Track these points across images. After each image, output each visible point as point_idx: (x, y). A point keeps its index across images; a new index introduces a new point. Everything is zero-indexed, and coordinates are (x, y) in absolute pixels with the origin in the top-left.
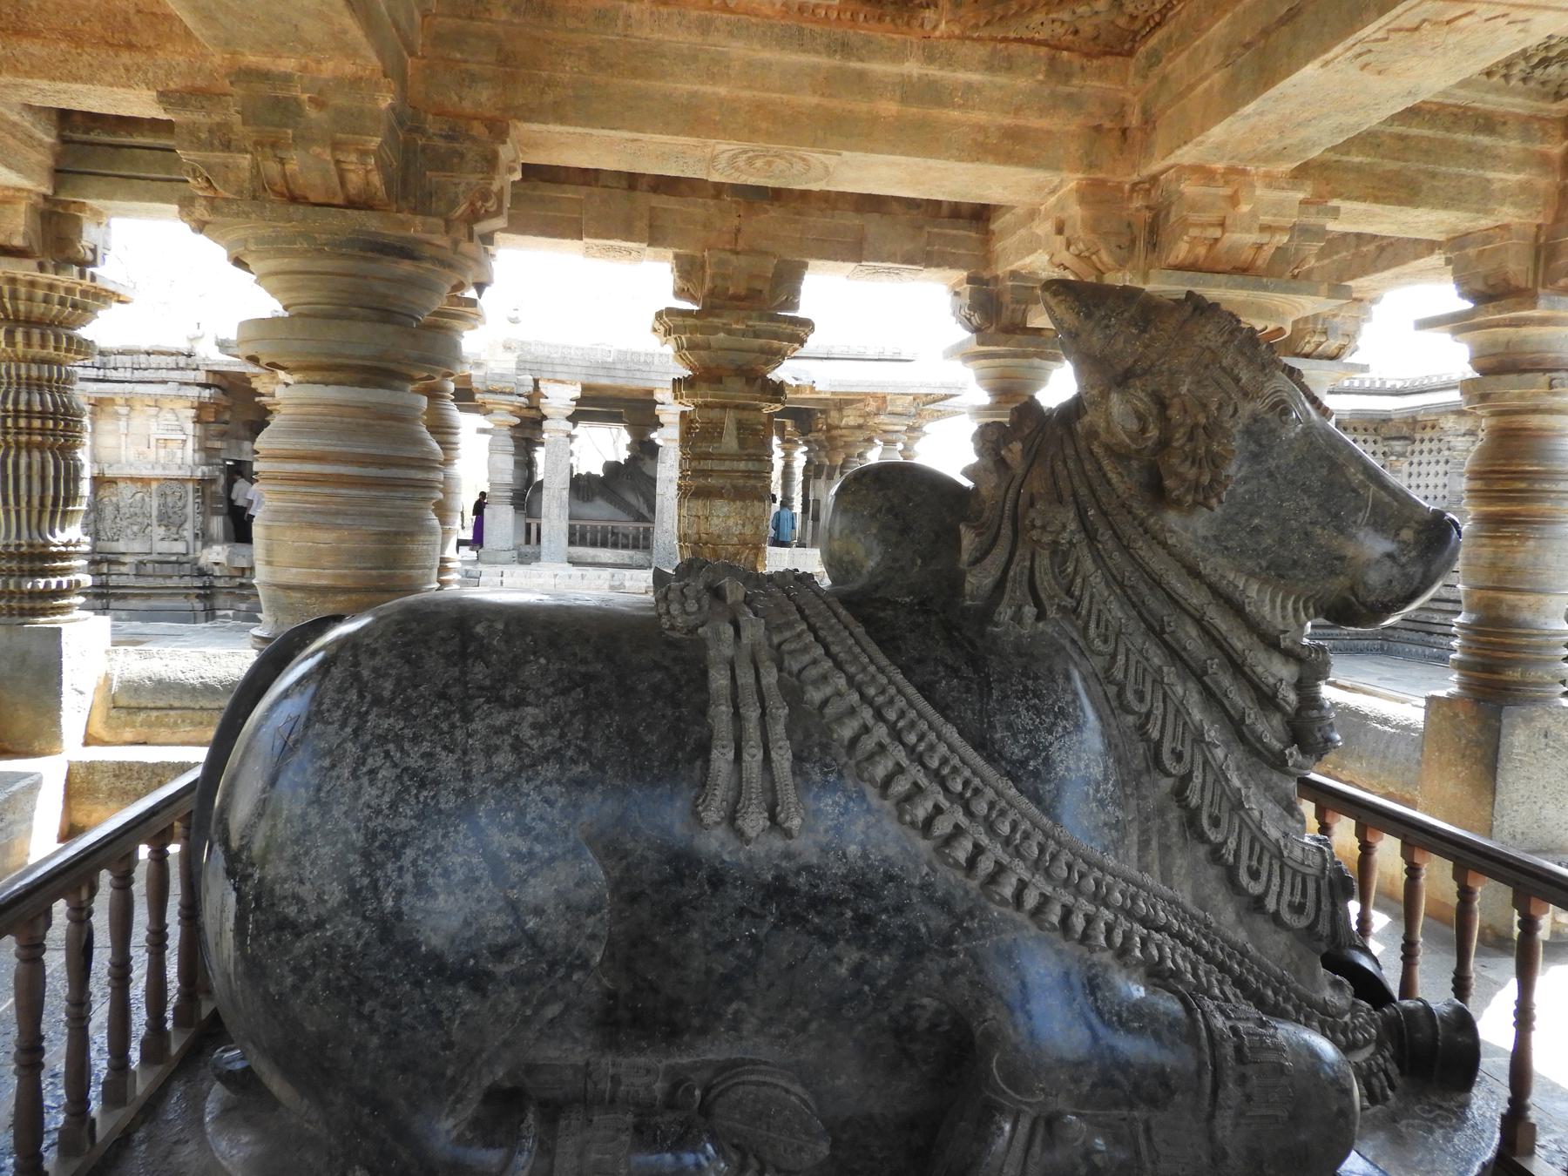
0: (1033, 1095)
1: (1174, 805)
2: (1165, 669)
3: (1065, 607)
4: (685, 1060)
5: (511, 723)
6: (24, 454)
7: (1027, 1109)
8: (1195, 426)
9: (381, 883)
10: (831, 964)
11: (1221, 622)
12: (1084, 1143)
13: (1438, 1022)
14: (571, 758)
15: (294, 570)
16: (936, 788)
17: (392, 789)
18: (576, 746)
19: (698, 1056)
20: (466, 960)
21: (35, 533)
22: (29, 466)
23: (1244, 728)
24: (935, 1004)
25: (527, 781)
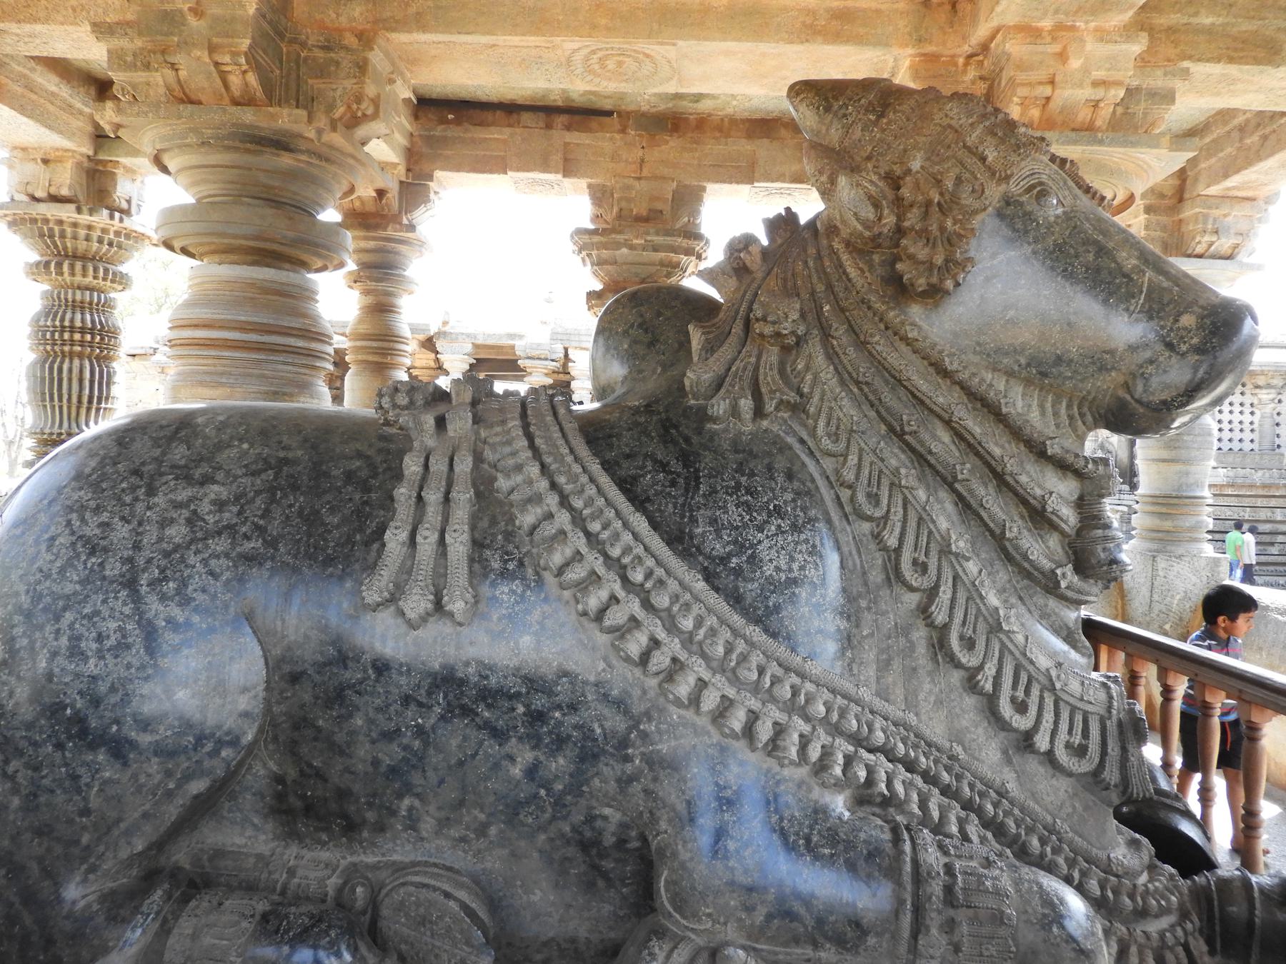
1: (920, 623)
2: (903, 471)
4: (370, 859)
5: (191, 500)
6: (67, 360)
7: (693, 936)
8: (928, 204)
9: (38, 644)
10: (504, 763)
11: (975, 426)
13: (1256, 894)
16: (612, 576)
18: (253, 523)
19: (383, 855)
21: (74, 425)
22: (70, 370)
23: (1007, 544)
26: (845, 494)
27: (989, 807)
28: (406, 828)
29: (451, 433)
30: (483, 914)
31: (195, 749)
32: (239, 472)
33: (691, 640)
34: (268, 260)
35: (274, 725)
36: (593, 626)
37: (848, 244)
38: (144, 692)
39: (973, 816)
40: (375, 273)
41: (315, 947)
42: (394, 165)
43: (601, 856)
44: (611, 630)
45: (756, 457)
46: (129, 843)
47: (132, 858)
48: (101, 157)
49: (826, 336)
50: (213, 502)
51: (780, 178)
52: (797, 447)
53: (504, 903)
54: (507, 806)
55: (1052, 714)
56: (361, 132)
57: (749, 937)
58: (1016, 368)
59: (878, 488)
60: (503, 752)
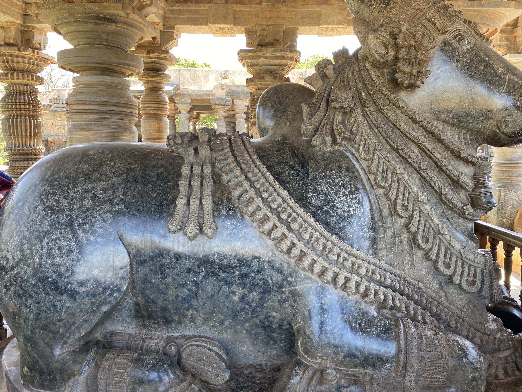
0: (316, 359)
1: (405, 231)
2: (398, 166)
3: (347, 138)
4: (175, 334)
6: (19, 117)
8: (410, 46)
9: (34, 252)
11: (429, 145)
12: (337, 382)
14: (116, 203)
19: (181, 333)
20: (67, 285)
22: (21, 122)
23: (443, 196)
24: (279, 316)
25: (96, 212)
27: (434, 308)
28: (190, 322)
29: (201, 155)
30: (224, 356)
31: (103, 294)
32: (111, 176)
33: (308, 243)
34: (108, 73)
36: (266, 238)
37: (372, 64)
39: (427, 312)
40: (152, 73)
41: (158, 372)
42: (157, 24)
43: (272, 332)
44: (274, 239)
45: (333, 162)
46: (79, 332)
49: (363, 106)
50: (102, 189)
51: (332, 23)
52: (351, 157)
53: (231, 351)
54: (232, 312)
56: (145, 12)
57: (336, 365)
58: (448, 119)
60: (230, 291)
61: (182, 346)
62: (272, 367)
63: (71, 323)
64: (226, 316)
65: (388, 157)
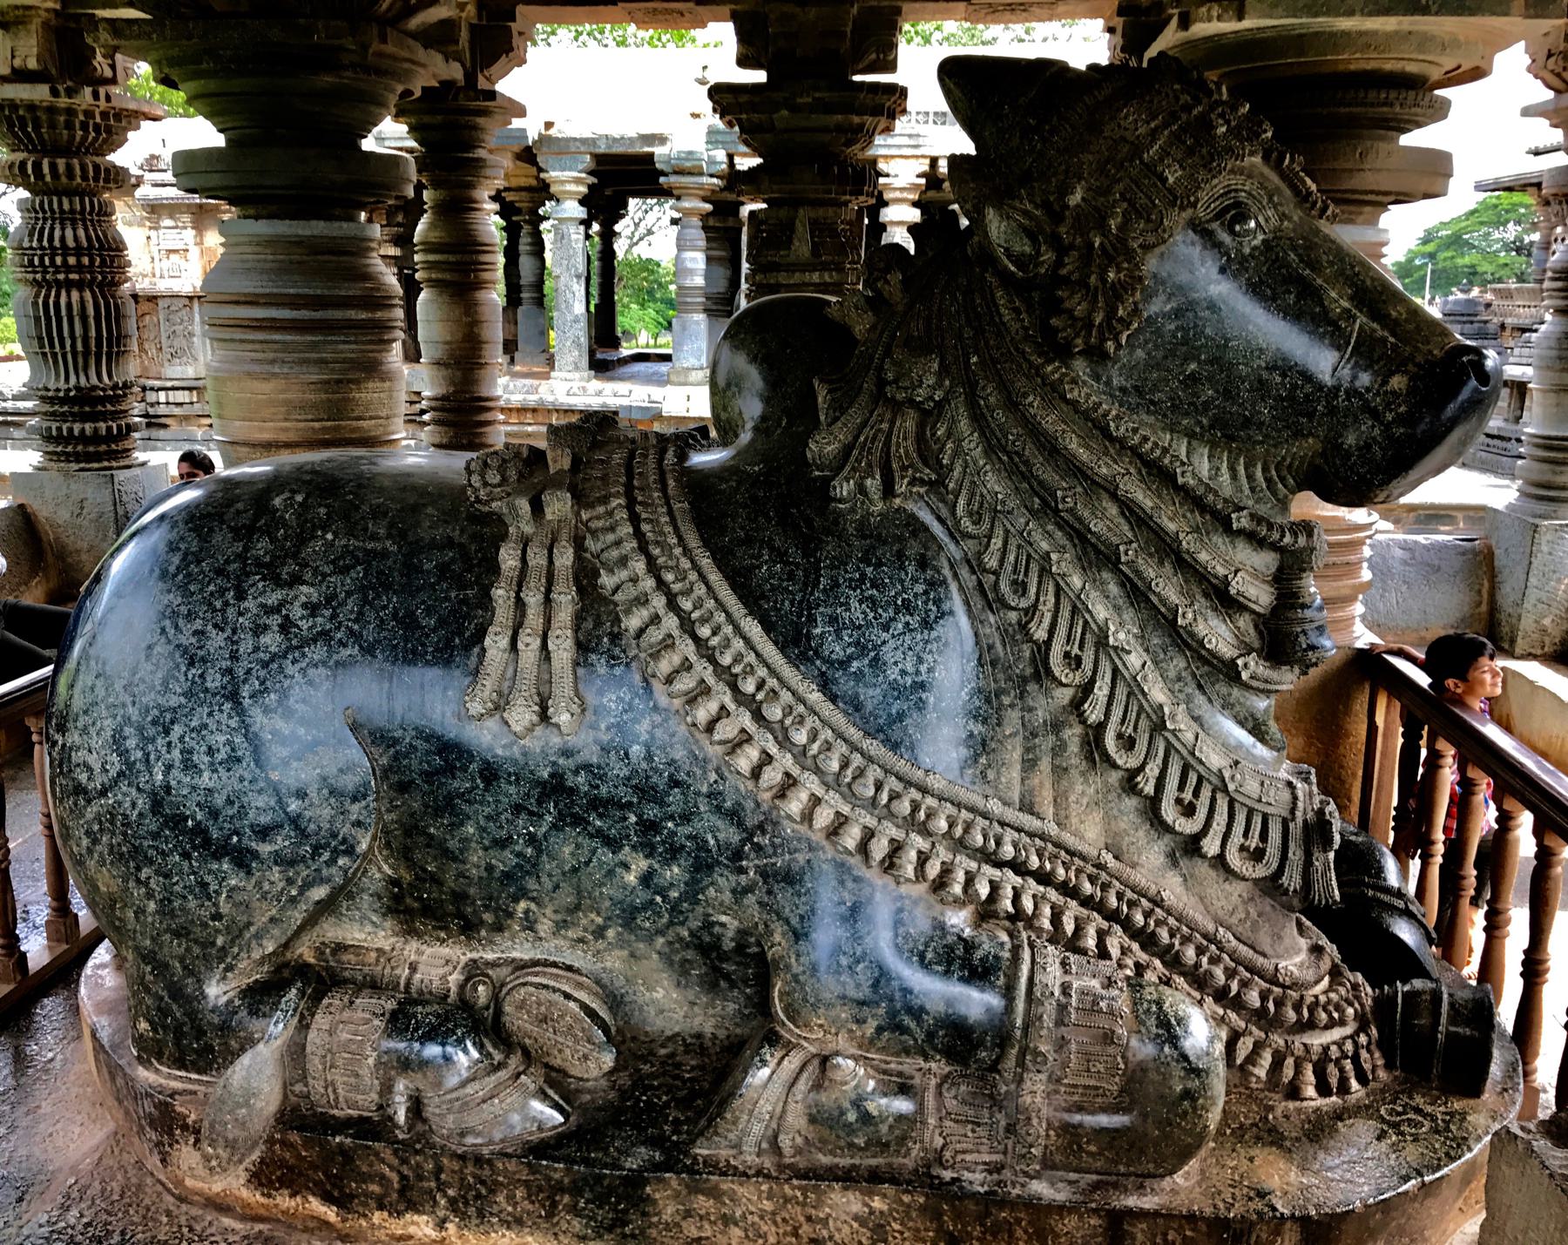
1: (1073, 719)
2: (1054, 556)
4: (490, 956)
5: (283, 603)
9: (152, 757)
15: (238, 423)
17: (166, 665)
20: (230, 837)
24: (736, 923)
26: (989, 579)
28: (524, 929)
29: (549, 517)
30: (604, 1013)
32: (327, 570)
33: (804, 753)
35: (386, 832)
36: (703, 738)
38: (260, 804)
41: (443, 1045)
43: (722, 960)
44: (721, 743)
45: (885, 543)
47: (263, 959)
48: (72, 11)
50: (305, 606)
52: (937, 528)
53: (627, 999)
54: (624, 911)
55: (1225, 816)
57: (860, 1047)
59: (1026, 574)
61: (502, 985)
62: (726, 1043)
63: (241, 925)
64: (609, 918)
65: (1029, 534)
